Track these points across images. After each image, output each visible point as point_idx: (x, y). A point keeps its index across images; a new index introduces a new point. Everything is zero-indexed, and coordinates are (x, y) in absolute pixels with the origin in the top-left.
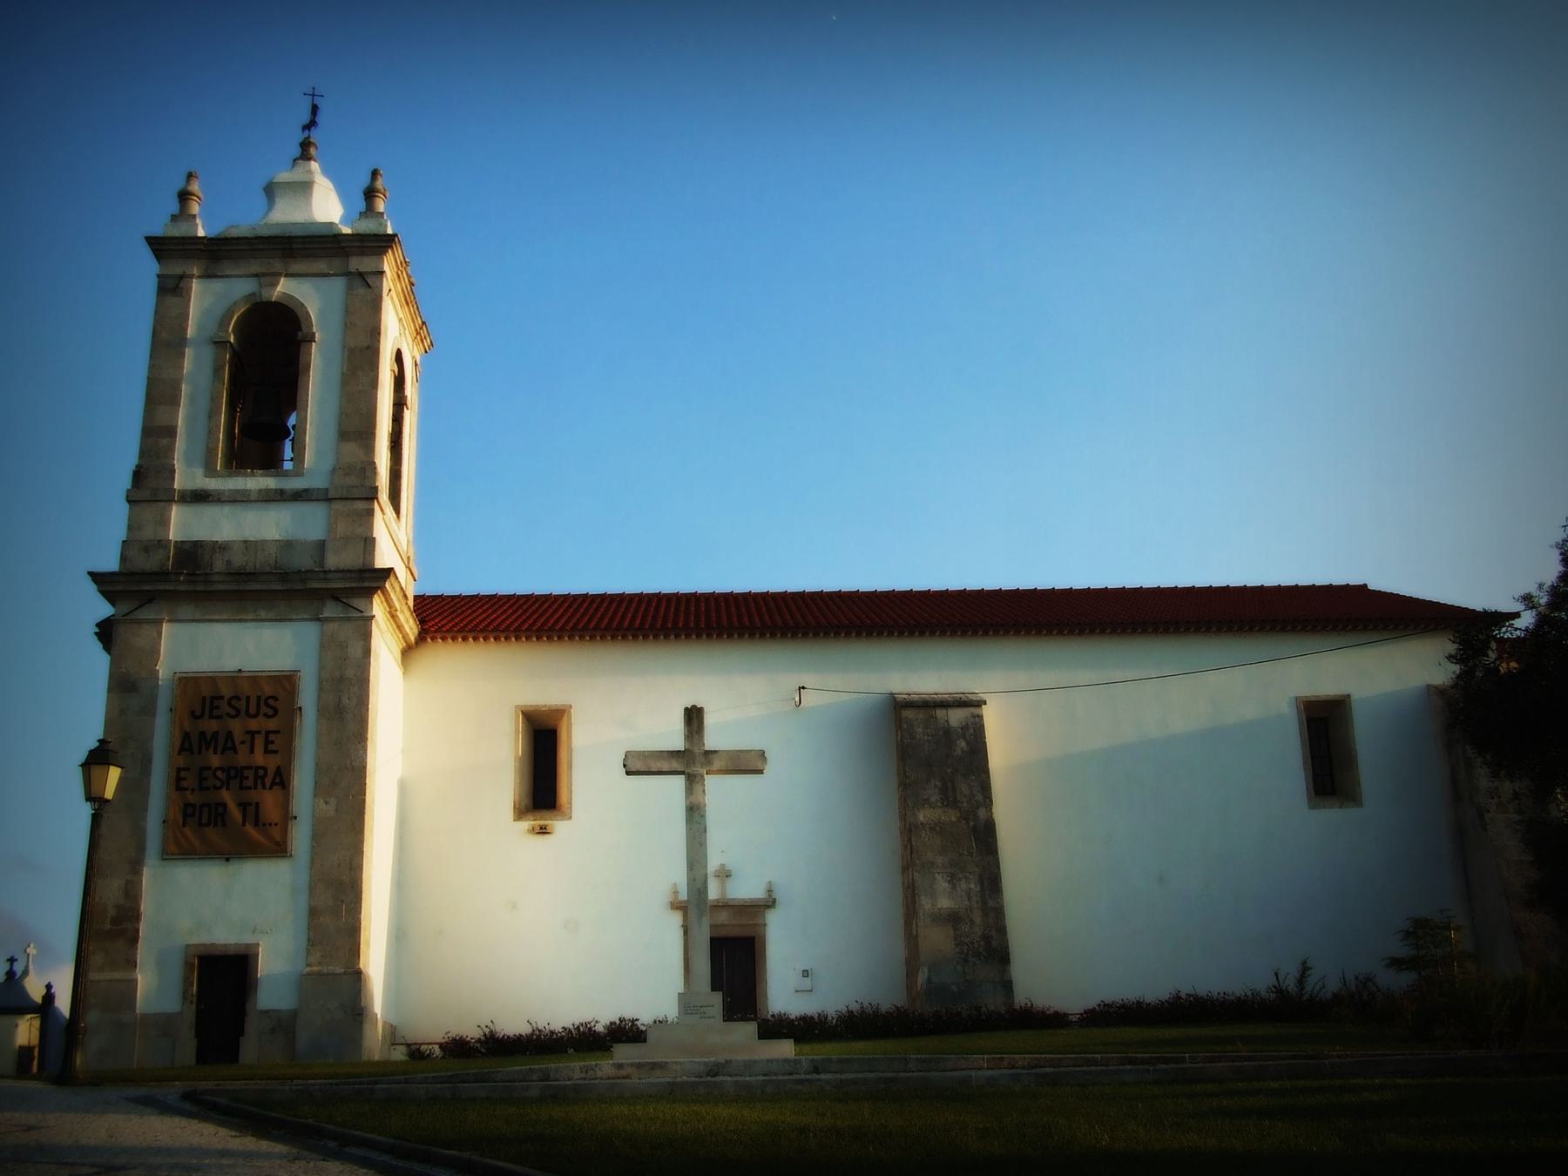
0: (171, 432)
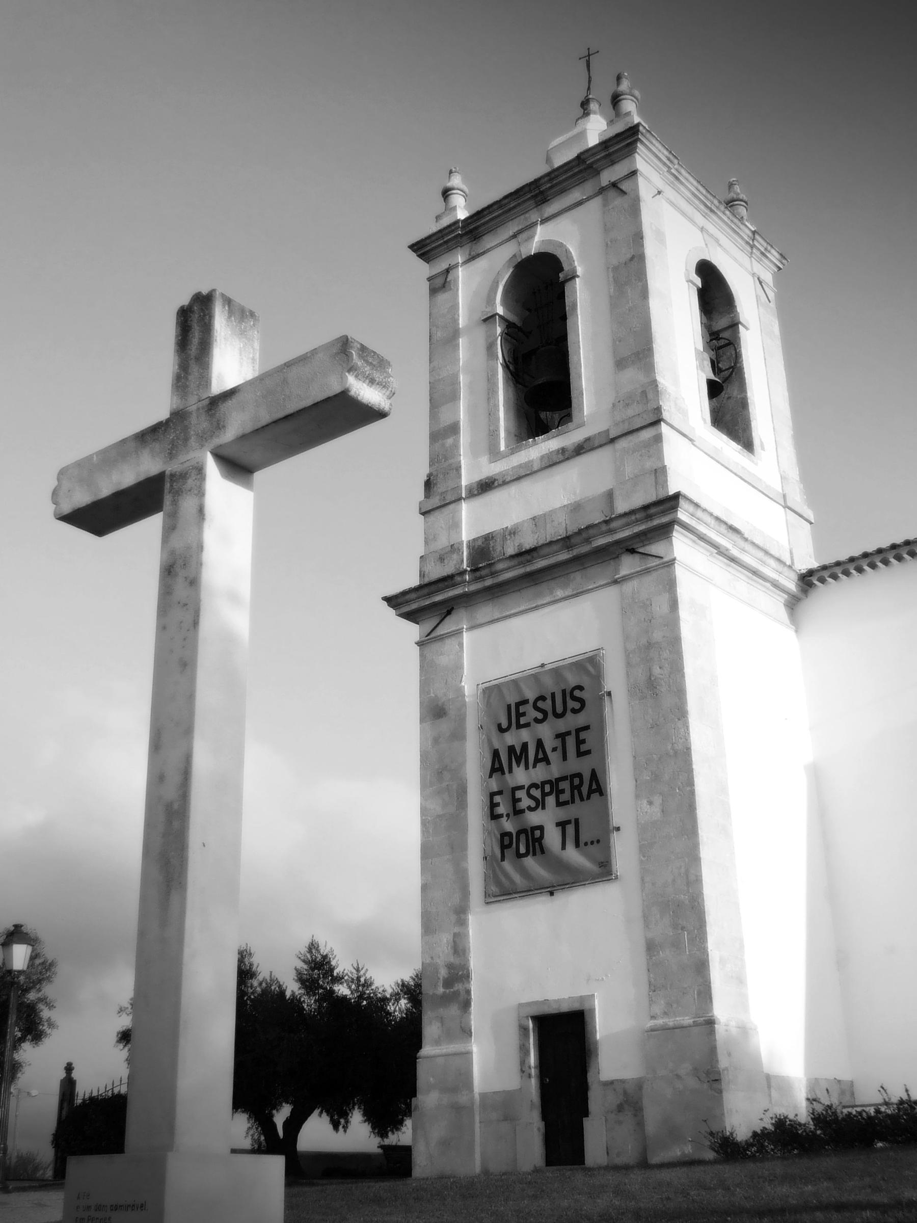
0: (454, 429)
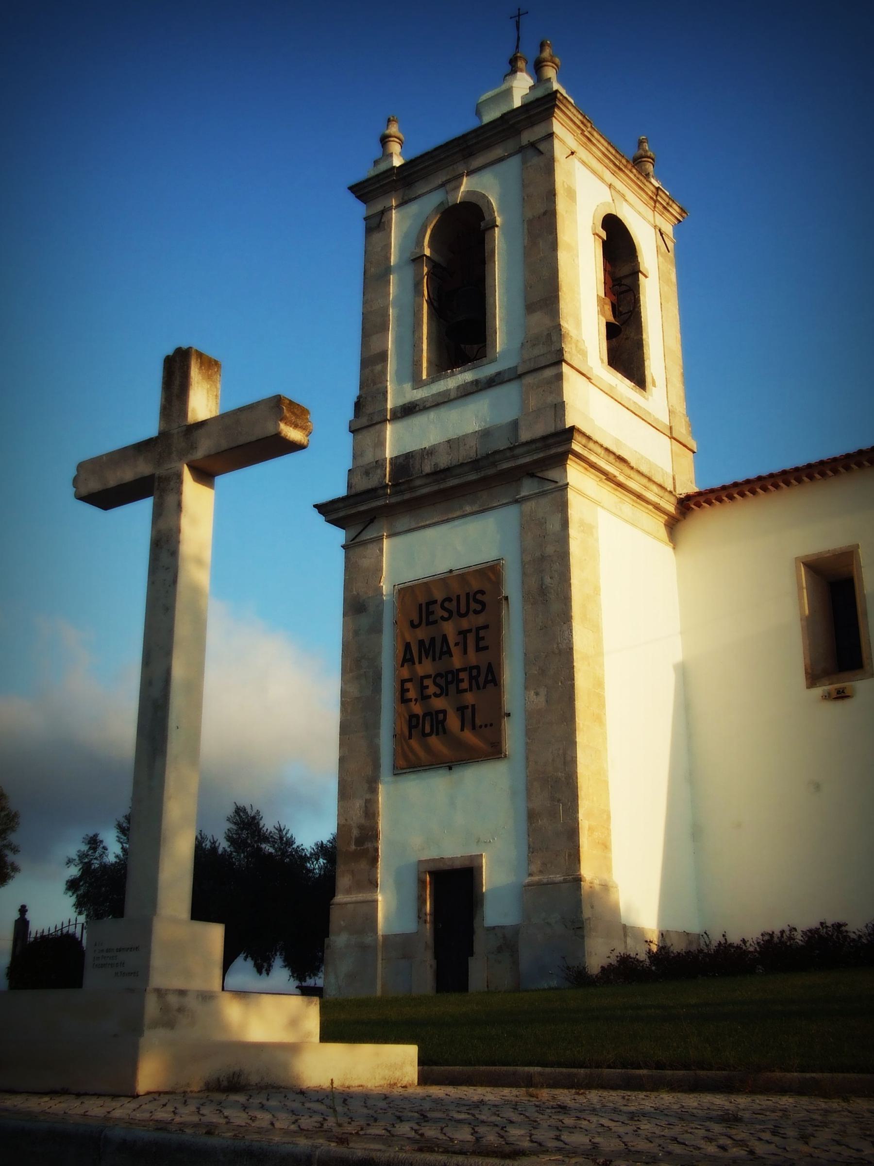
0: (383, 357)
